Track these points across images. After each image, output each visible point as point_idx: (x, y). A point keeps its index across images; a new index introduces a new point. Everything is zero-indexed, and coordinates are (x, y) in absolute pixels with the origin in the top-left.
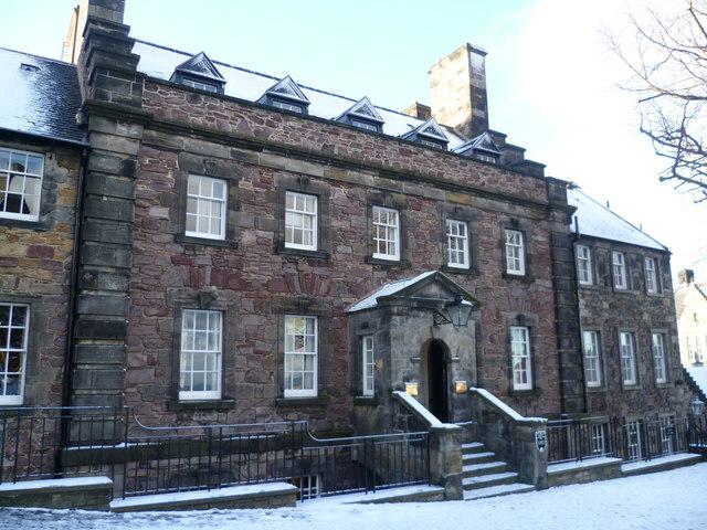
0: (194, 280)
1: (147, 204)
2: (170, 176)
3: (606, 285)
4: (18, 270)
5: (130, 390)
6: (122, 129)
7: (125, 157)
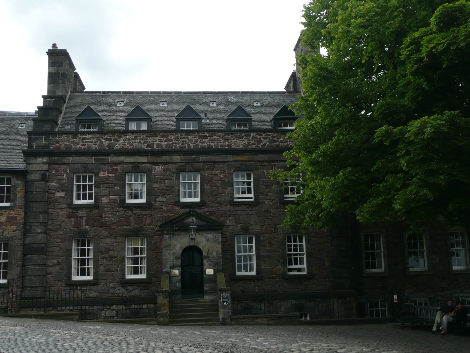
0: (78, 225)
1: (54, 192)
2: (65, 177)
4: (3, 227)
5: (49, 276)
6: (40, 160)
7: (43, 172)
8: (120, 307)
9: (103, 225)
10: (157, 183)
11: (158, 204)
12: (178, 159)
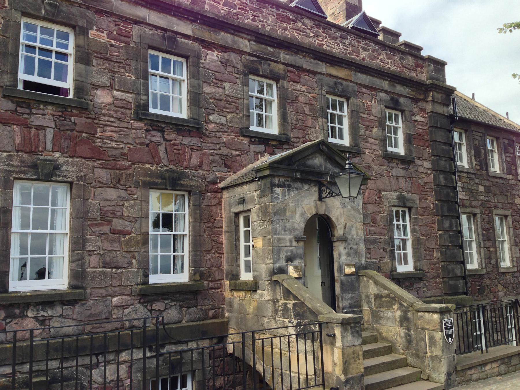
0: (30, 147)
3: (482, 169)
8: (138, 354)
9: (97, 155)
10: (209, 83)
11: (211, 126)
12: (246, 46)
